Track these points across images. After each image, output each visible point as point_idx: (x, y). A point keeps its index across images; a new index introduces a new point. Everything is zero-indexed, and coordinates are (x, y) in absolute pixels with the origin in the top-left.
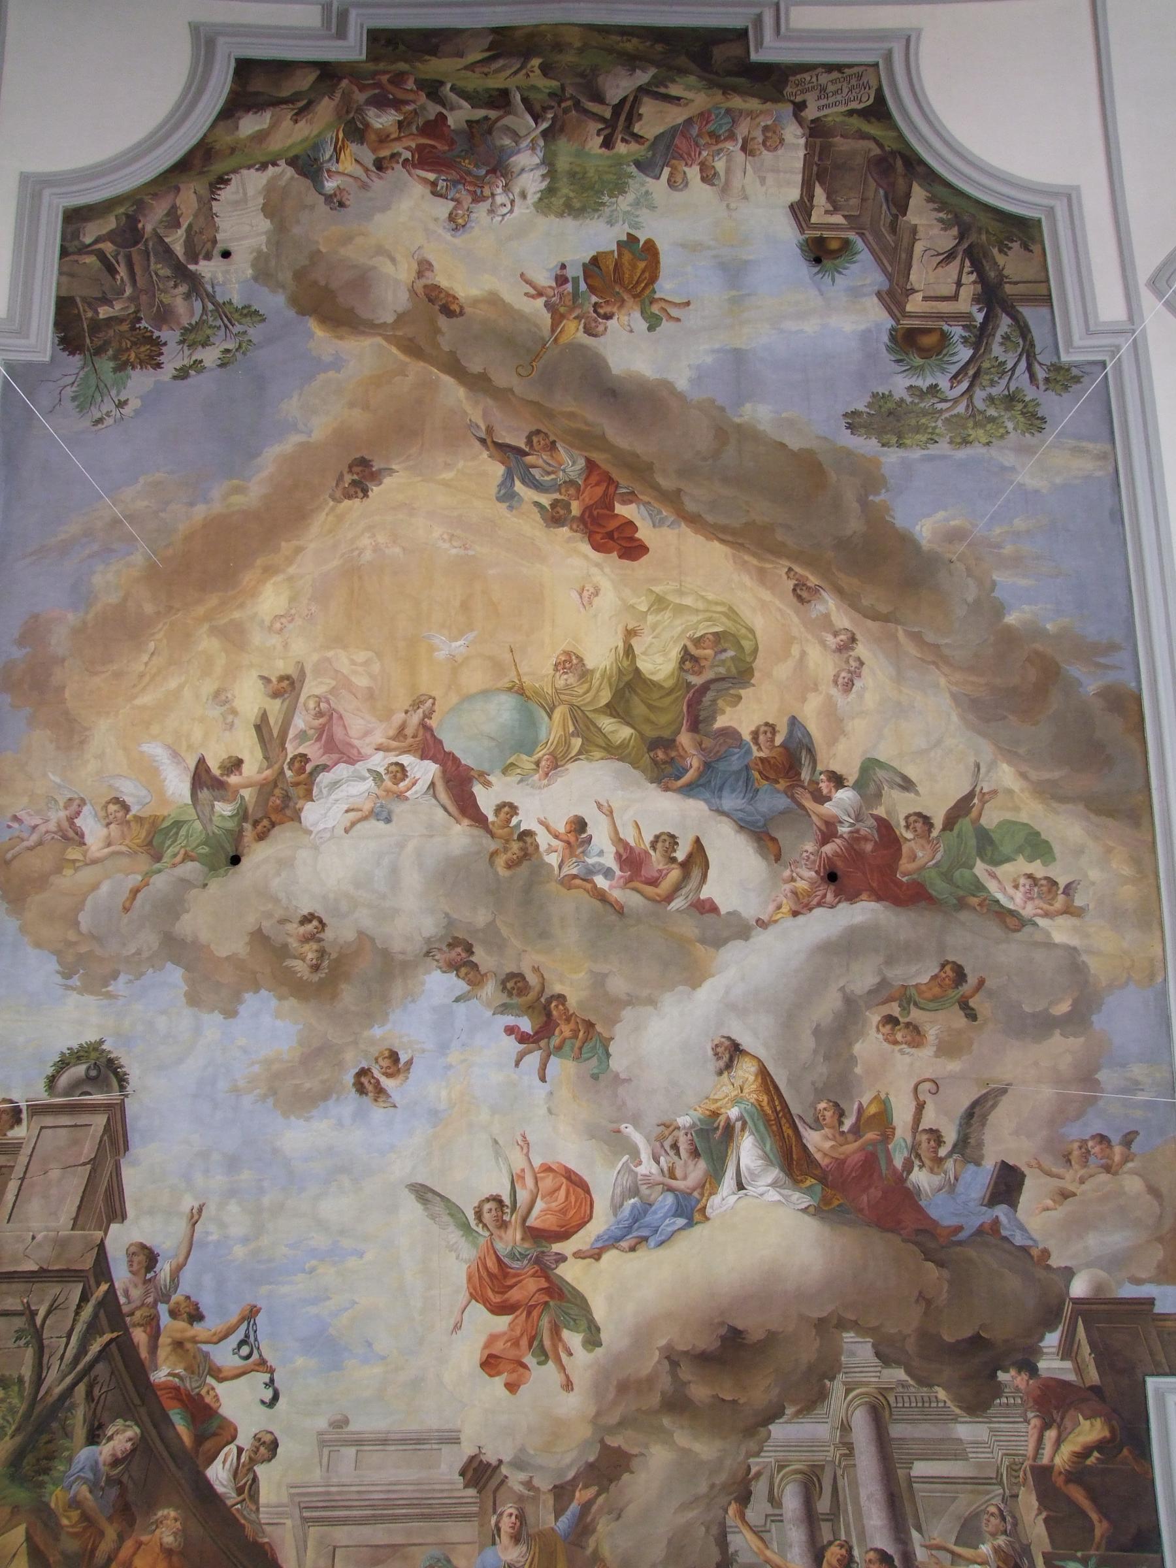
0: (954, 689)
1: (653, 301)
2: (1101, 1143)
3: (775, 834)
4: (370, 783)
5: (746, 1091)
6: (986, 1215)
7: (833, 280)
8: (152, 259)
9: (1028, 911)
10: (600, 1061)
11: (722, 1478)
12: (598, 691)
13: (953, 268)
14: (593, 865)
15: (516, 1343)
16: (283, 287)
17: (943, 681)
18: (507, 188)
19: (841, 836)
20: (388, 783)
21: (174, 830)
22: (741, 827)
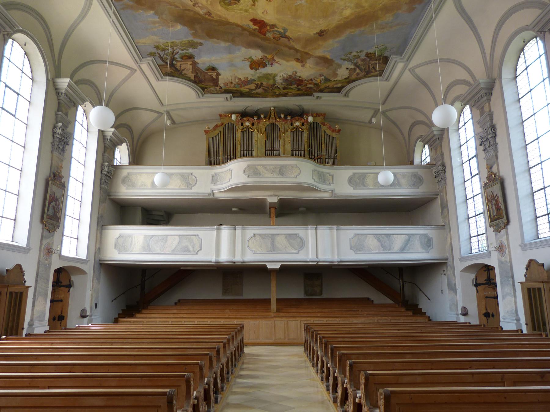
7: (209, 65)
8: (364, 69)
13: (182, 68)
18: (284, 77)
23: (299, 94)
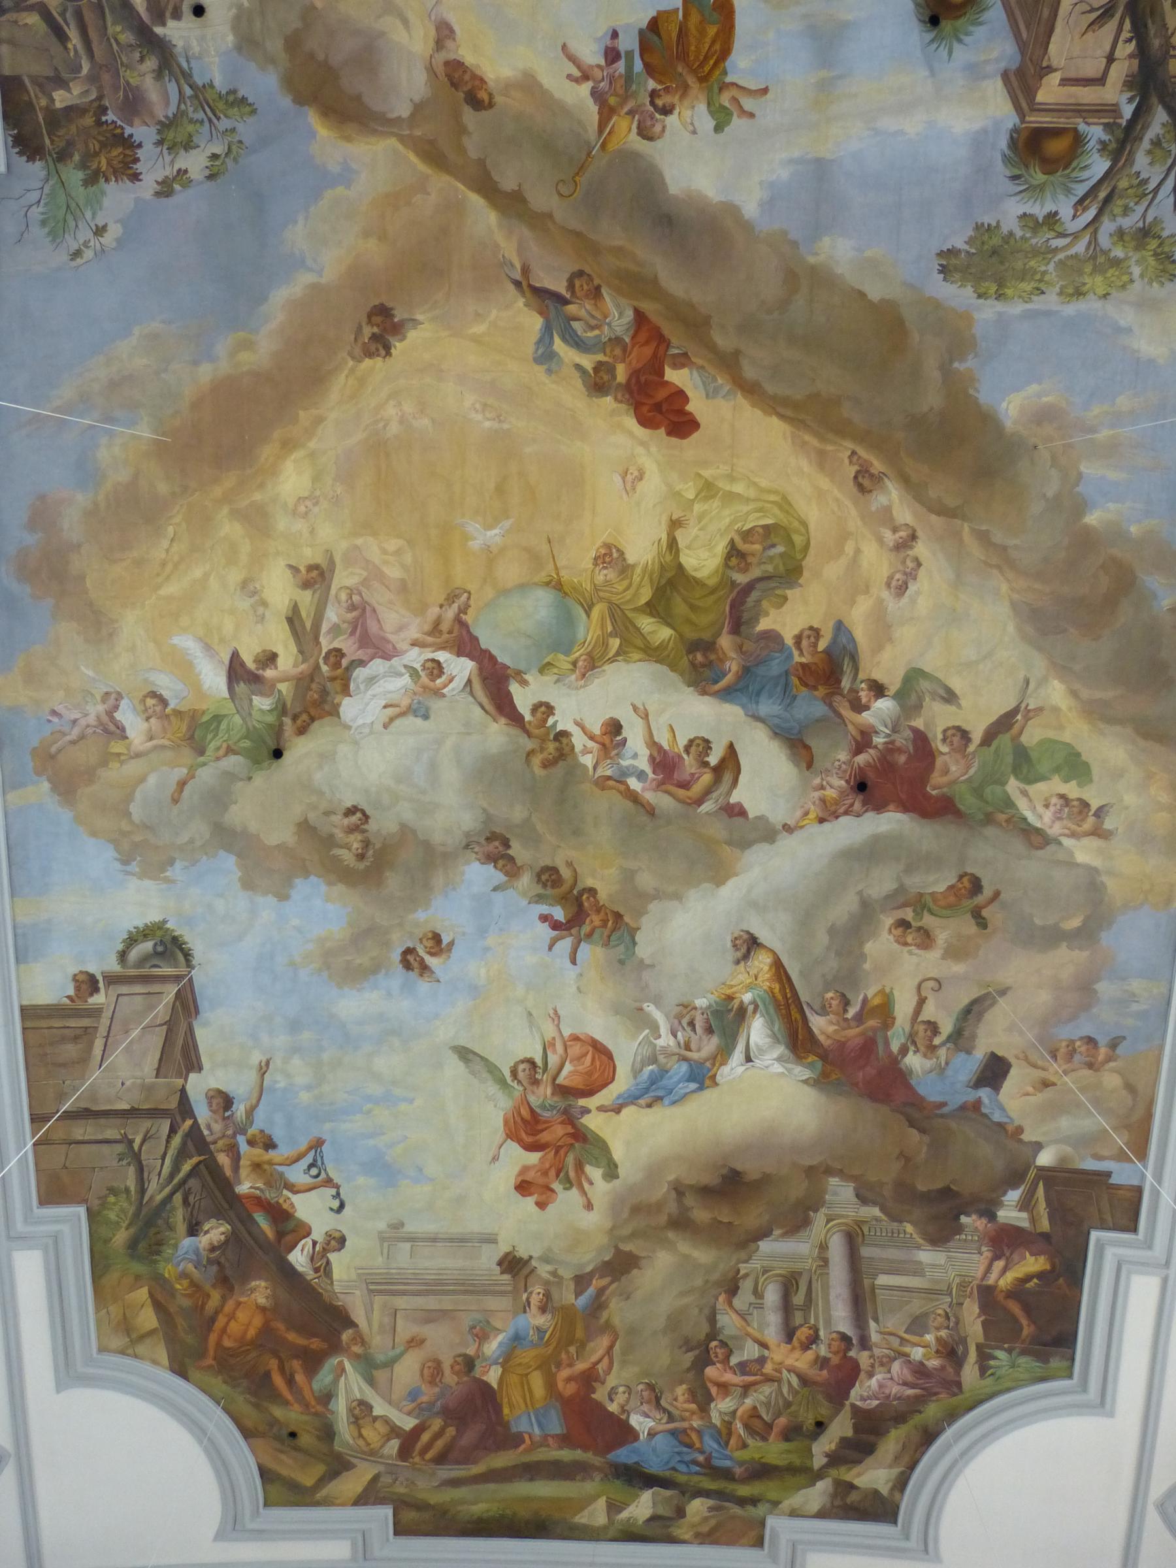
0: (1016, 596)
1: (723, 87)
2: (1088, 1043)
3: (808, 742)
4: (406, 680)
5: (760, 979)
6: (971, 1096)
7: (950, 53)
9: (1055, 830)
10: (627, 949)
11: (716, 1276)
12: (640, 586)
14: (627, 768)
15: (545, 1173)
16: (272, 61)
17: (1004, 588)
19: (876, 747)
20: (425, 679)
21: (215, 725)
22: (776, 734)
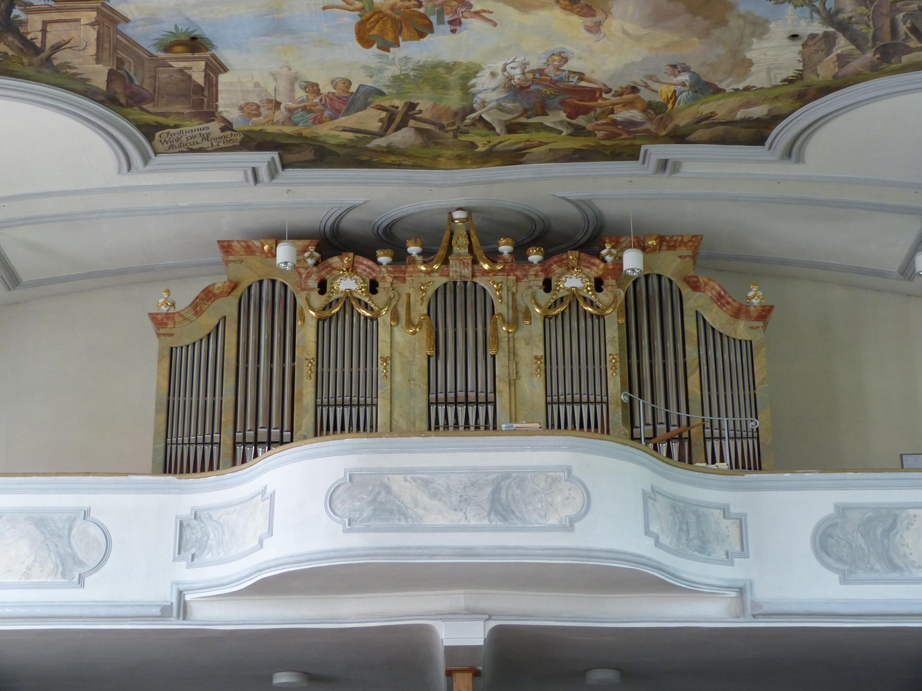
7: (176, 27)
8: (870, 36)
13: (51, 40)
16: (739, 16)
18: (510, 78)
23: (576, 151)
